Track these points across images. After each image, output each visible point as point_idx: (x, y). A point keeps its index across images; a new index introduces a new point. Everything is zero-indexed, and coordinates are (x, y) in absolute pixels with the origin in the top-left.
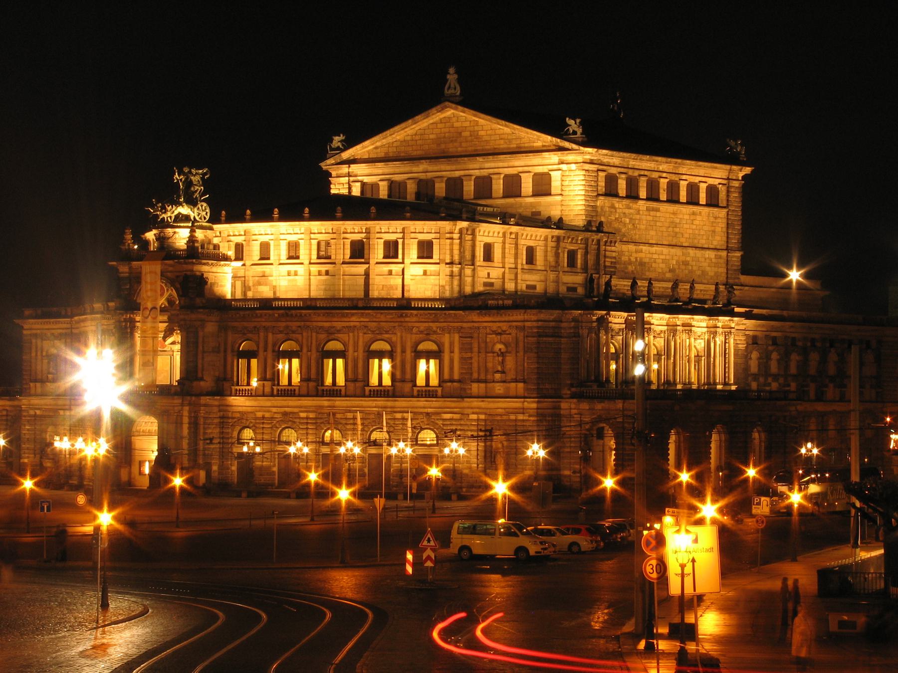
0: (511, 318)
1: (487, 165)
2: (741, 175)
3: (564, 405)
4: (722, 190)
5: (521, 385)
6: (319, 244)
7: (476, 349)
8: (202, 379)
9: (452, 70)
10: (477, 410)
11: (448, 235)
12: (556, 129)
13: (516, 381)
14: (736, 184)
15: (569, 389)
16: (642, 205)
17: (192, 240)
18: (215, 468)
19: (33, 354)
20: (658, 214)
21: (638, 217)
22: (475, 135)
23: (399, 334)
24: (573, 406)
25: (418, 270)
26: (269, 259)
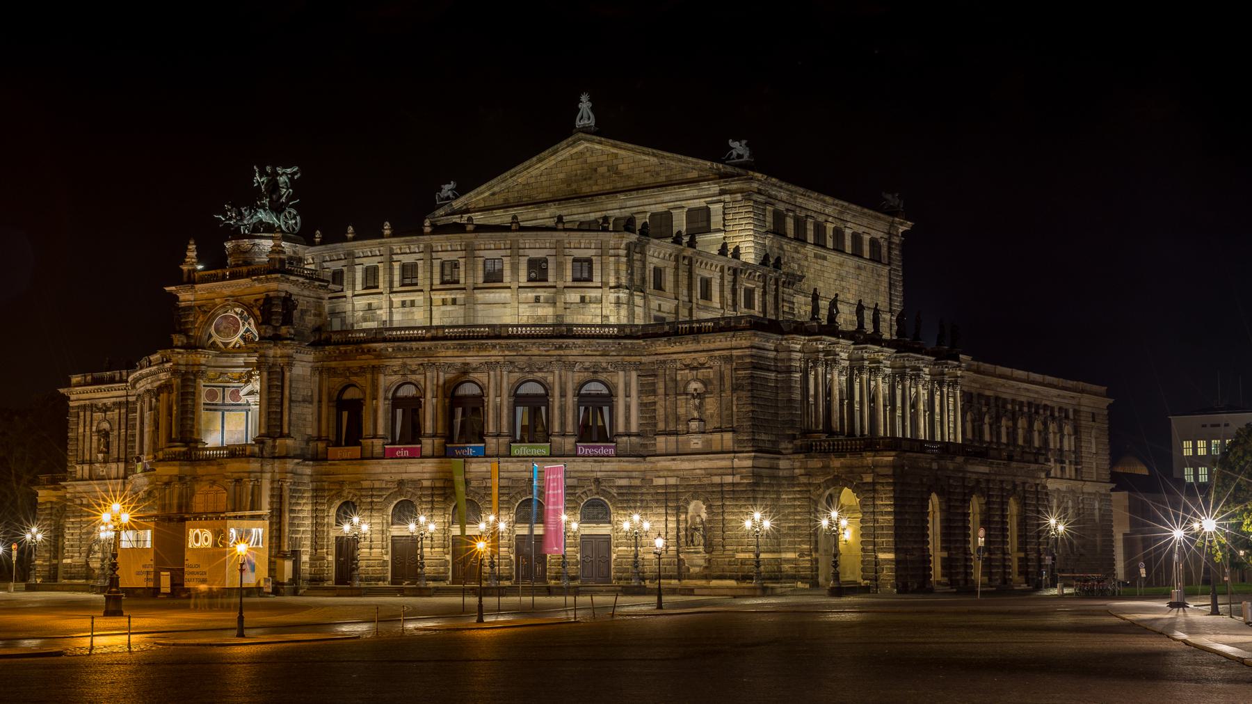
0: (712, 346)
1: (629, 203)
2: (901, 229)
3: (783, 464)
4: (884, 243)
5: (728, 436)
6: (442, 265)
7: (661, 391)
8: (289, 436)
9: (584, 98)
10: (666, 473)
11: (612, 252)
12: (717, 152)
13: (721, 430)
14: (896, 240)
15: (791, 442)
16: (810, 250)
17: (277, 250)
18: (305, 558)
19: (81, 430)
20: (825, 263)
21: (806, 263)
22: (613, 169)
23: (557, 372)
24: (797, 464)
25: (574, 297)
26: (377, 287)
